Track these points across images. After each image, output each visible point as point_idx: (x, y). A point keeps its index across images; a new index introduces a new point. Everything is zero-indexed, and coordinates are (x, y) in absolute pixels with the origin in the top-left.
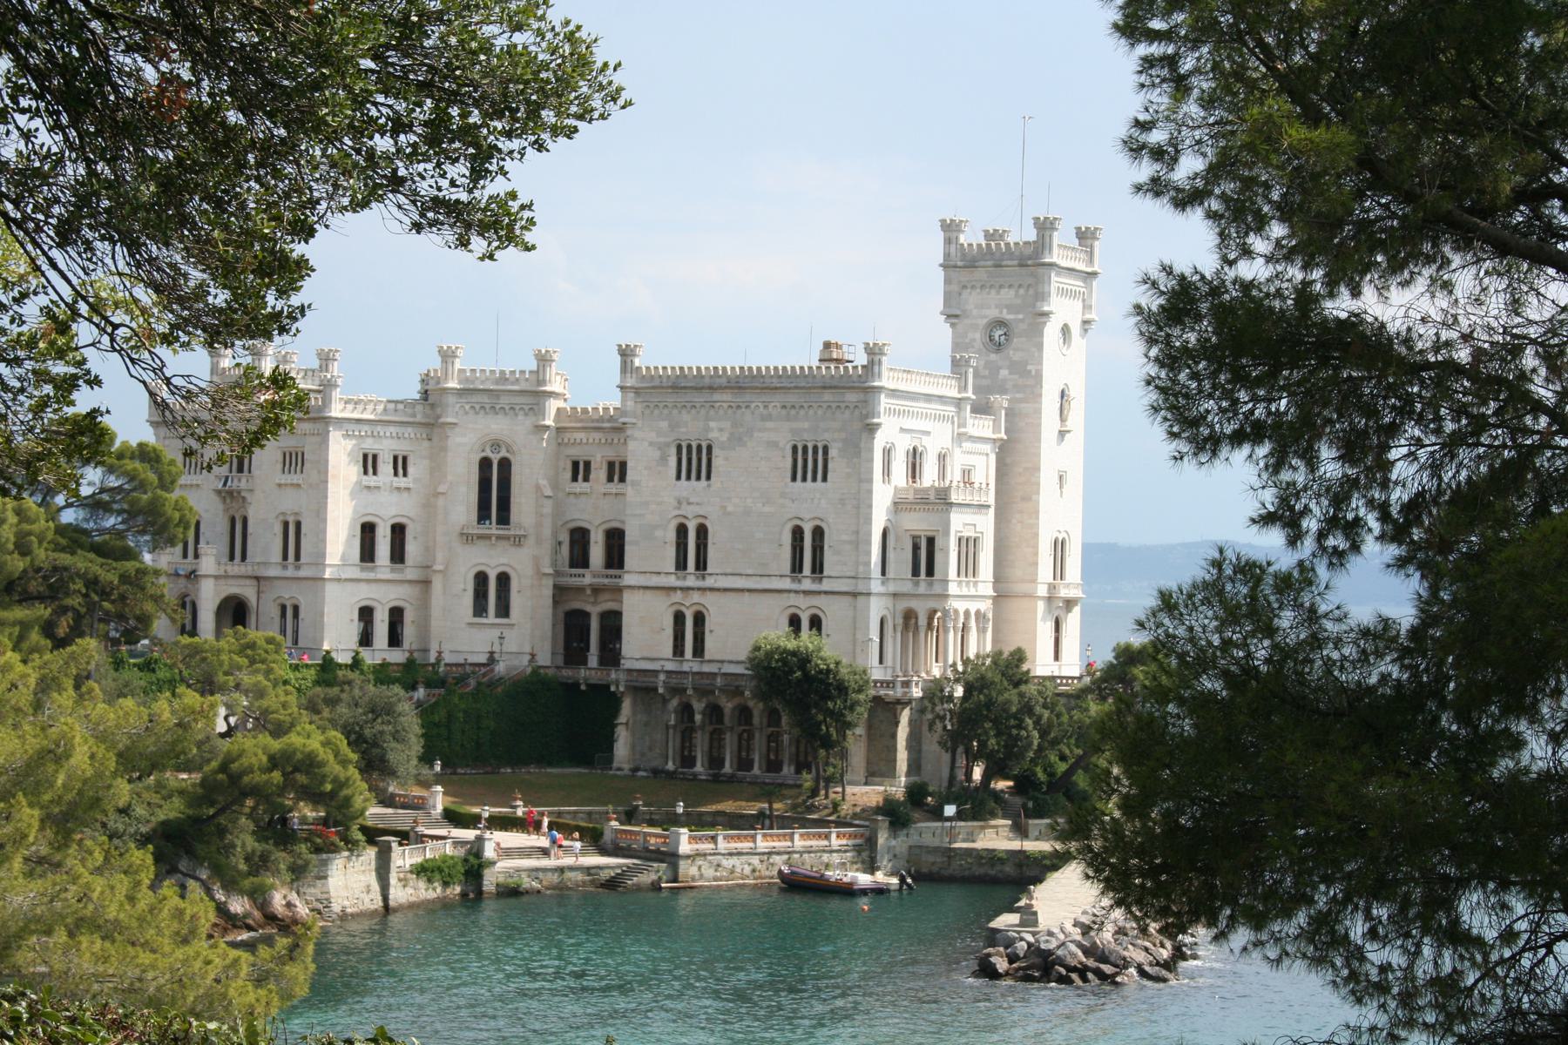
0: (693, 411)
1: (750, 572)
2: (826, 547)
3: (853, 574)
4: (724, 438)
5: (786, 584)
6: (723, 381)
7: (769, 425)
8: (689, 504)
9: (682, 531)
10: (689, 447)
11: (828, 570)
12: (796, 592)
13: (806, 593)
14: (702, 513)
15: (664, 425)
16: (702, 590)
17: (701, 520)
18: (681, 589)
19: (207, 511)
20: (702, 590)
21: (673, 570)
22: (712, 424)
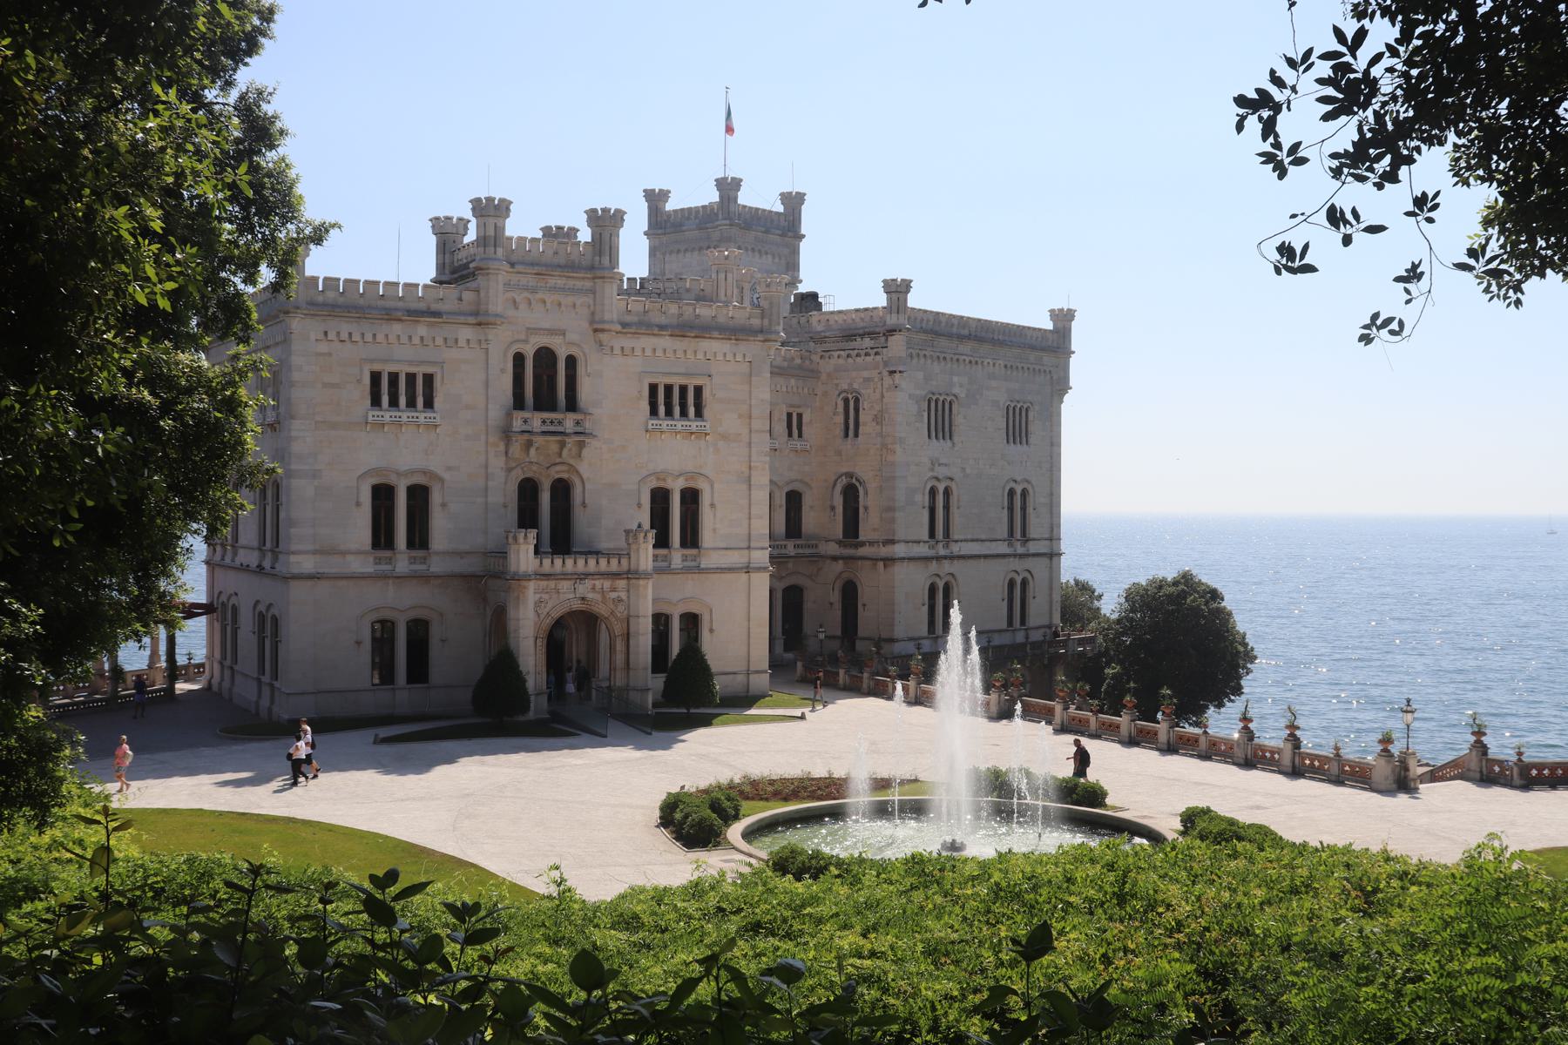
0: (943, 363)
1: (983, 537)
2: (1030, 510)
3: (1047, 536)
4: (963, 395)
5: (1003, 548)
6: (966, 332)
7: (994, 383)
8: (939, 465)
9: (933, 492)
10: (937, 401)
11: (1033, 532)
12: (1015, 556)
13: (1022, 556)
14: (949, 475)
15: (920, 375)
16: (952, 558)
17: (948, 483)
18: (938, 558)
19: (449, 469)
20: (952, 558)
21: (925, 536)
22: (955, 379)
